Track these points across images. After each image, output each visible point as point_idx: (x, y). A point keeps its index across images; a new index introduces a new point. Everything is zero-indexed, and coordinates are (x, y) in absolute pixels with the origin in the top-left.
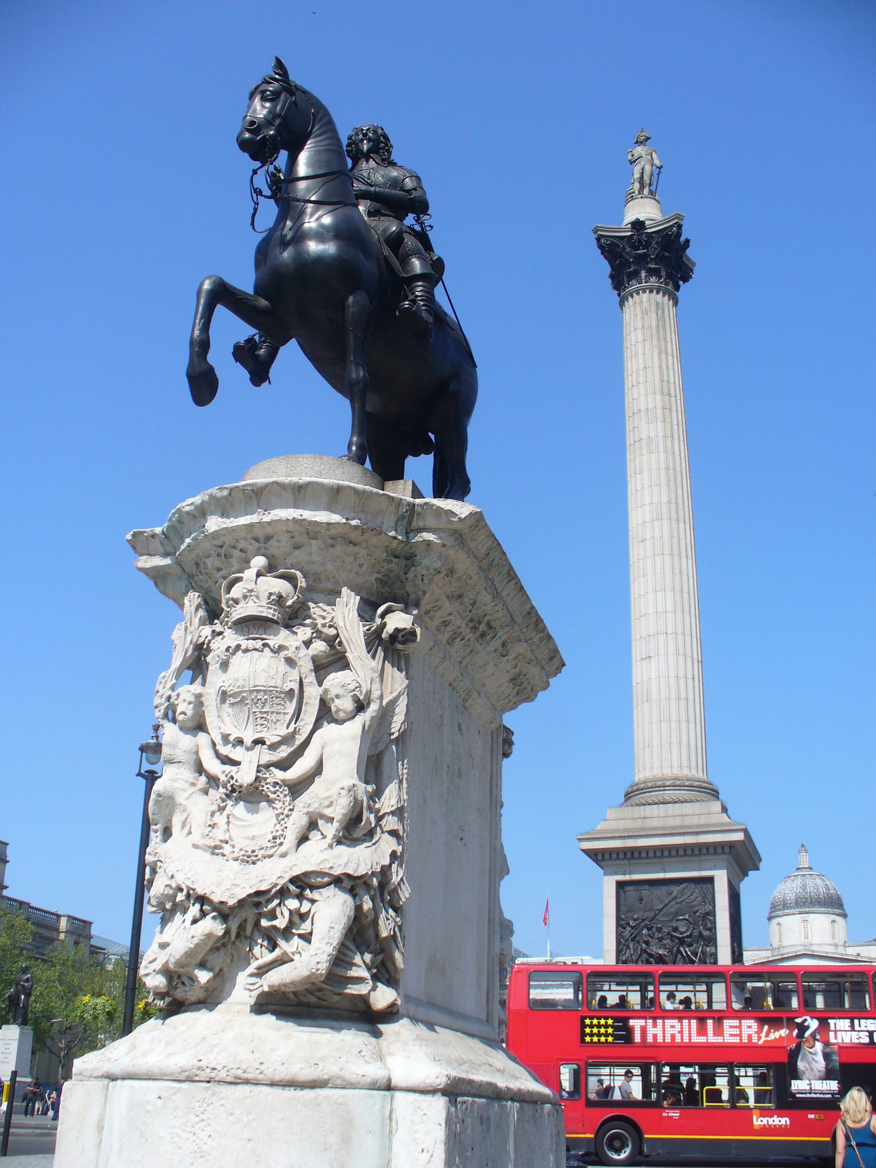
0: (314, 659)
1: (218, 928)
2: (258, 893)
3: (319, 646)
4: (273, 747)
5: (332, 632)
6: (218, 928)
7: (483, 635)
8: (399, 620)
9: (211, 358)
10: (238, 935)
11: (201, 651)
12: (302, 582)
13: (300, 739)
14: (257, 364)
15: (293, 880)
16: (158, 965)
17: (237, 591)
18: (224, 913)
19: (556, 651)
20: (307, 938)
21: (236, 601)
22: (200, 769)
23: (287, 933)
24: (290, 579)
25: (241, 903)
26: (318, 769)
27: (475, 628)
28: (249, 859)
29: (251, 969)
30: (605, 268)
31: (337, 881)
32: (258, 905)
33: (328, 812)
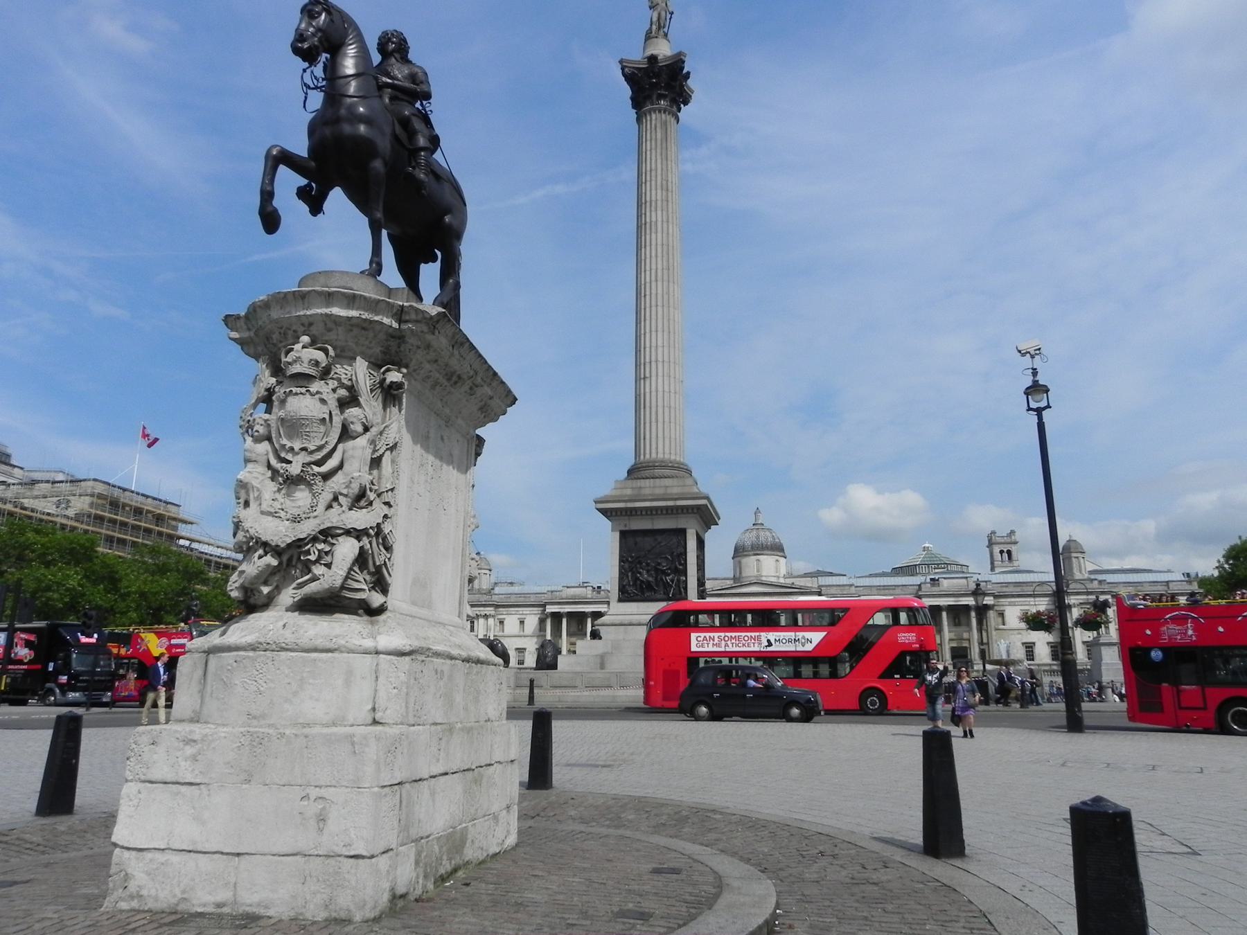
0: (339, 400)
1: (275, 562)
2: (300, 540)
3: (343, 392)
4: (312, 452)
5: (349, 383)
6: (275, 562)
7: (456, 383)
8: (394, 376)
9: (276, 203)
10: (288, 565)
11: (270, 392)
12: (332, 353)
13: (329, 447)
14: (314, 201)
15: (321, 532)
16: (237, 585)
17: (289, 359)
18: (277, 551)
19: (509, 391)
20: (328, 566)
21: (290, 363)
22: (269, 466)
23: (317, 561)
24: (326, 352)
25: (289, 546)
26: (341, 466)
27: (449, 380)
28: (296, 520)
29: (294, 585)
30: (627, 91)
31: (348, 532)
32: (300, 547)
33: (345, 492)
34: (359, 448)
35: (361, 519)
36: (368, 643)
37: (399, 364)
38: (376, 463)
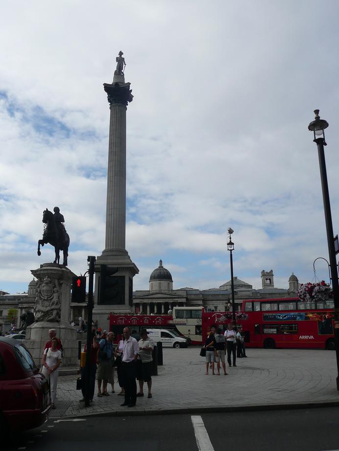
3: (53, 285)
8: (61, 282)
26: (53, 298)
28: (46, 307)
34: (55, 295)
35: (57, 307)
36: (58, 327)
37: (62, 279)
38: (59, 297)
